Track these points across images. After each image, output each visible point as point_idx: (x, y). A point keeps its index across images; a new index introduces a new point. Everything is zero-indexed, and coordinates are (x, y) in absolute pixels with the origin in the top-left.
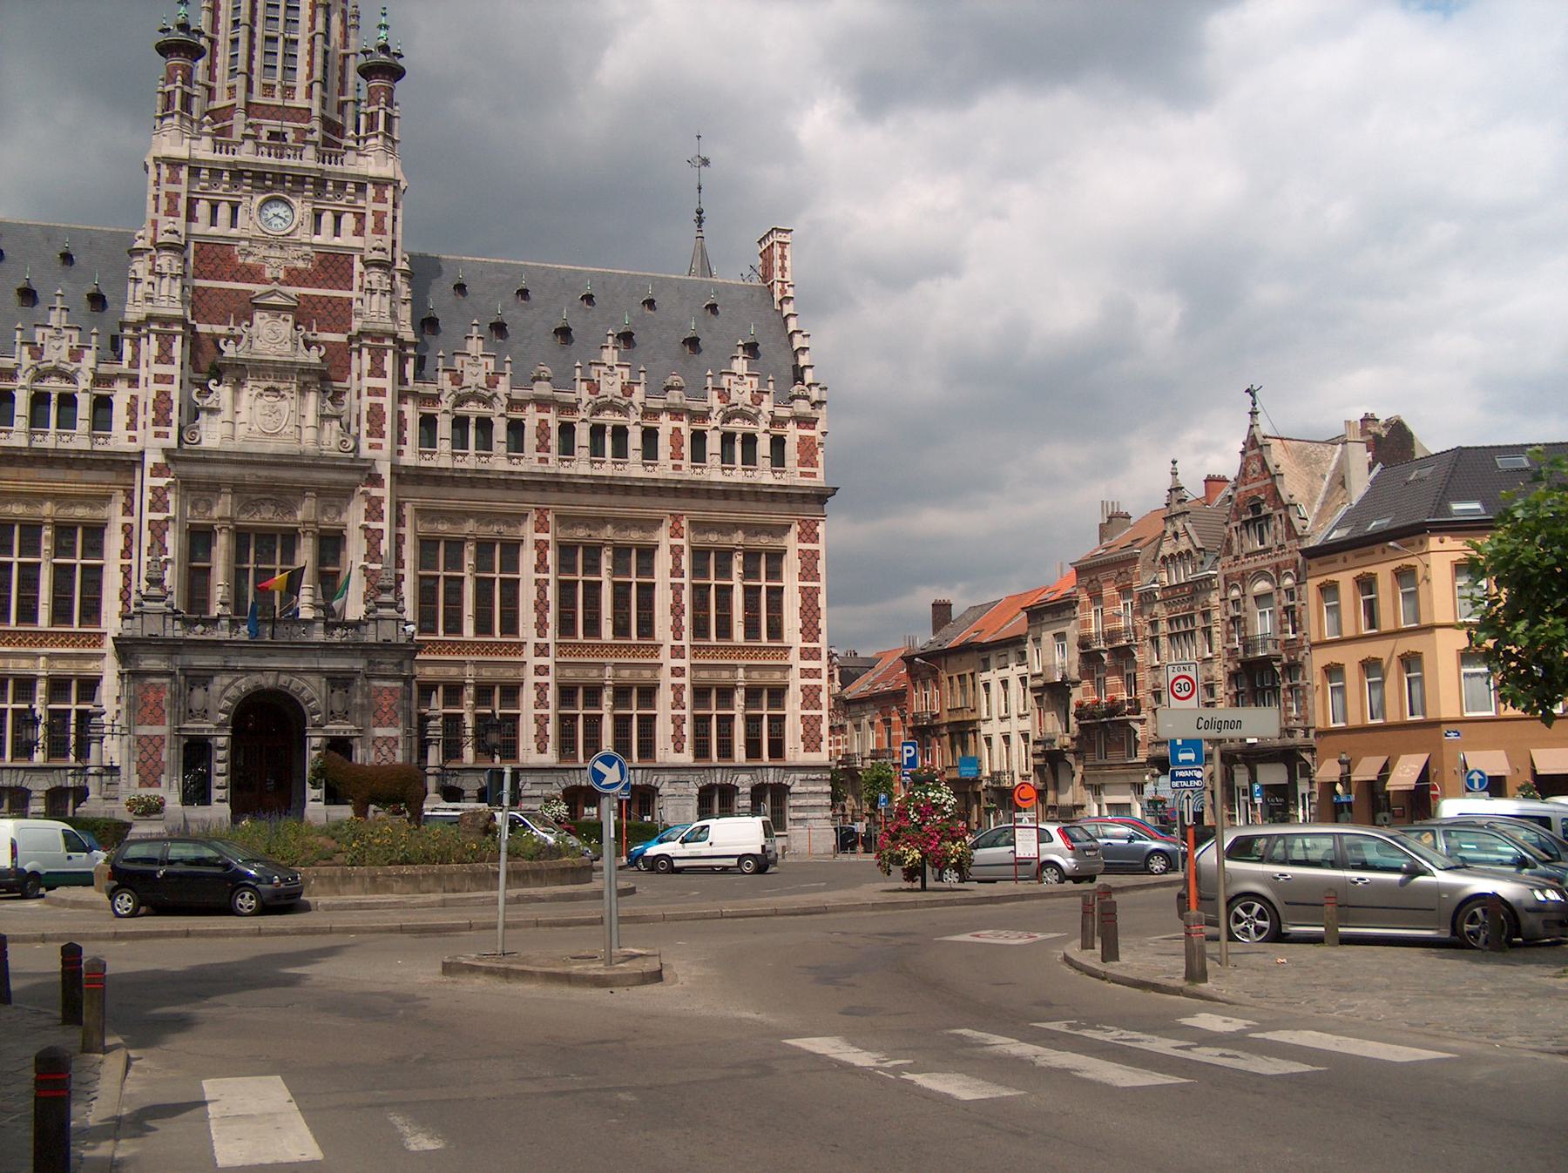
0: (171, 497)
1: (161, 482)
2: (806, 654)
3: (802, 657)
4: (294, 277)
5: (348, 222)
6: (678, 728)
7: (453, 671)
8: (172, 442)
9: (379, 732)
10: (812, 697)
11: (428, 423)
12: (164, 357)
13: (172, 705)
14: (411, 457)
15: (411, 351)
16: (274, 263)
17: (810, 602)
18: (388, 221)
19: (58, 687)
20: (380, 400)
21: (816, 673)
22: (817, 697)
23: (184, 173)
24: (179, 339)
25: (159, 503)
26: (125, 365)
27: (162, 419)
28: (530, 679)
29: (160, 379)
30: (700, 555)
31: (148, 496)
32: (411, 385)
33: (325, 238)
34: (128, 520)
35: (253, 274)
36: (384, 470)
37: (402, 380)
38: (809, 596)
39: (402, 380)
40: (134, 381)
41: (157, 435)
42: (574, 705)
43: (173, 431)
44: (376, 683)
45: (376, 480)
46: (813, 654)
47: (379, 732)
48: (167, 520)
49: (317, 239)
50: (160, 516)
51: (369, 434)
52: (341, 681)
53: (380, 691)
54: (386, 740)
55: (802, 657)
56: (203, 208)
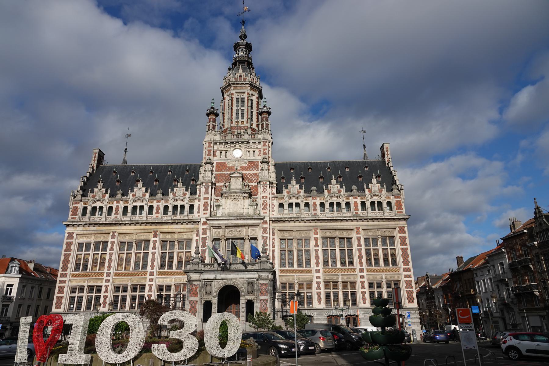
0: (208, 231)
1: (205, 227)
2: (405, 270)
3: (404, 271)
4: (243, 168)
5: (257, 152)
6: (364, 295)
7: (291, 278)
8: (208, 215)
9: (262, 298)
10: (409, 284)
12: (206, 192)
13: (201, 291)
14: (276, 214)
17: (405, 253)
18: (267, 151)
19: (134, 289)
20: (266, 199)
21: (409, 276)
22: (411, 284)
24: (210, 187)
25: (204, 233)
26: (197, 196)
27: (205, 209)
28: (315, 280)
29: (205, 198)
30: (367, 239)
31: (202, 231)
33: (251, 157)
34: (197, 238)
38: (404, 251)
40: (199, 200)
41: (204, 214)
42: (329, 288)
43: (208, 212)
44: (261, 282)
45: (265, 222)
46: (408, 270)
47: (262, 298)
48: (206, 238)
49: (248, 158)
50: (204, 236)
52: (250, 283)
53: (262, 284)
54: (264, 300)
55: (404, 271)
56: (218, 153)
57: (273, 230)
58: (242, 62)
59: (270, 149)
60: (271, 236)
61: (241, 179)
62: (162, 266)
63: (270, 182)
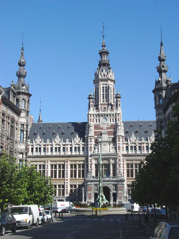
1: (91, 158)
4: (107, 128)
11: (127, 147)
15: (124, 137)
16: (105, 127)
18: (120, 119)
23: (92, 116)
32: (124, 142)
35: (102, 129)
36: (121, 155)
37: (123, 142)
39: (123, 142)
41: (90, 152)
43: (92, 151)
45: (119, 156)
50: (91, 163)
51: (118, 150)
54: (120, 193)
57: (123, 159)
58: (104, 65)
59: (121, 118)
60: (122, 163)
61: (107, 134)
62: (71, 176)
63: (121, 136)
